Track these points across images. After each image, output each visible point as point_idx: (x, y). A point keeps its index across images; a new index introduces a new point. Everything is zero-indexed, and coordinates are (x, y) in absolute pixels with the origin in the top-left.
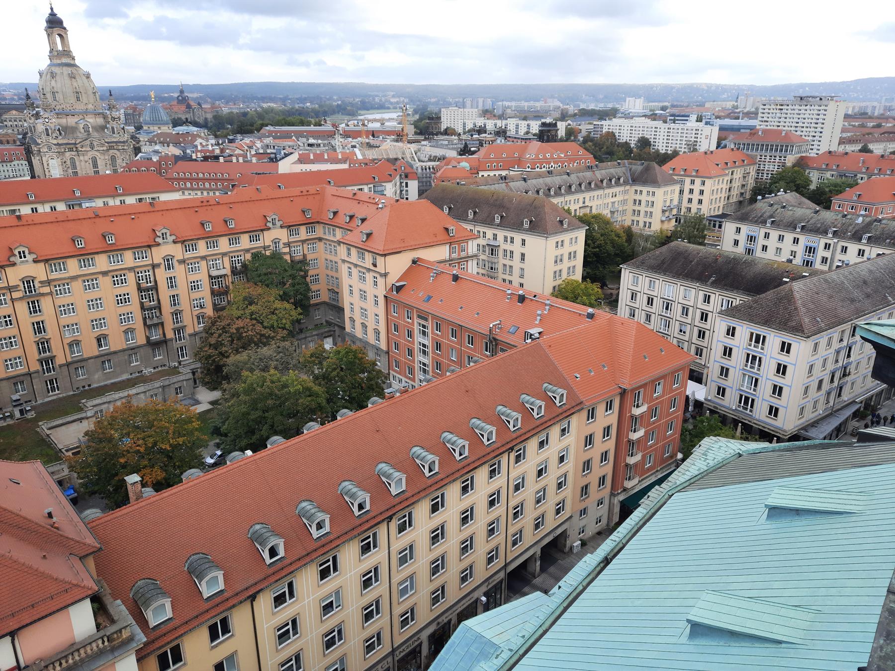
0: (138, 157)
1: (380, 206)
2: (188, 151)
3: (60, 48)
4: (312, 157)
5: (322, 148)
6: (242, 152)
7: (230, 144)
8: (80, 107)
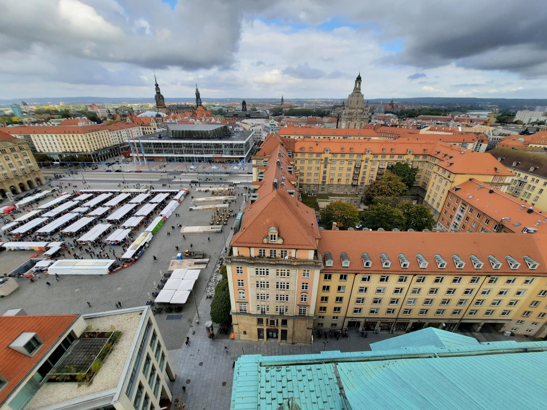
1: (462, 153)
2: (387, 123)
4: (436, 128)
5: (443, 125)
6: (407, 124)
8: (357, 106)
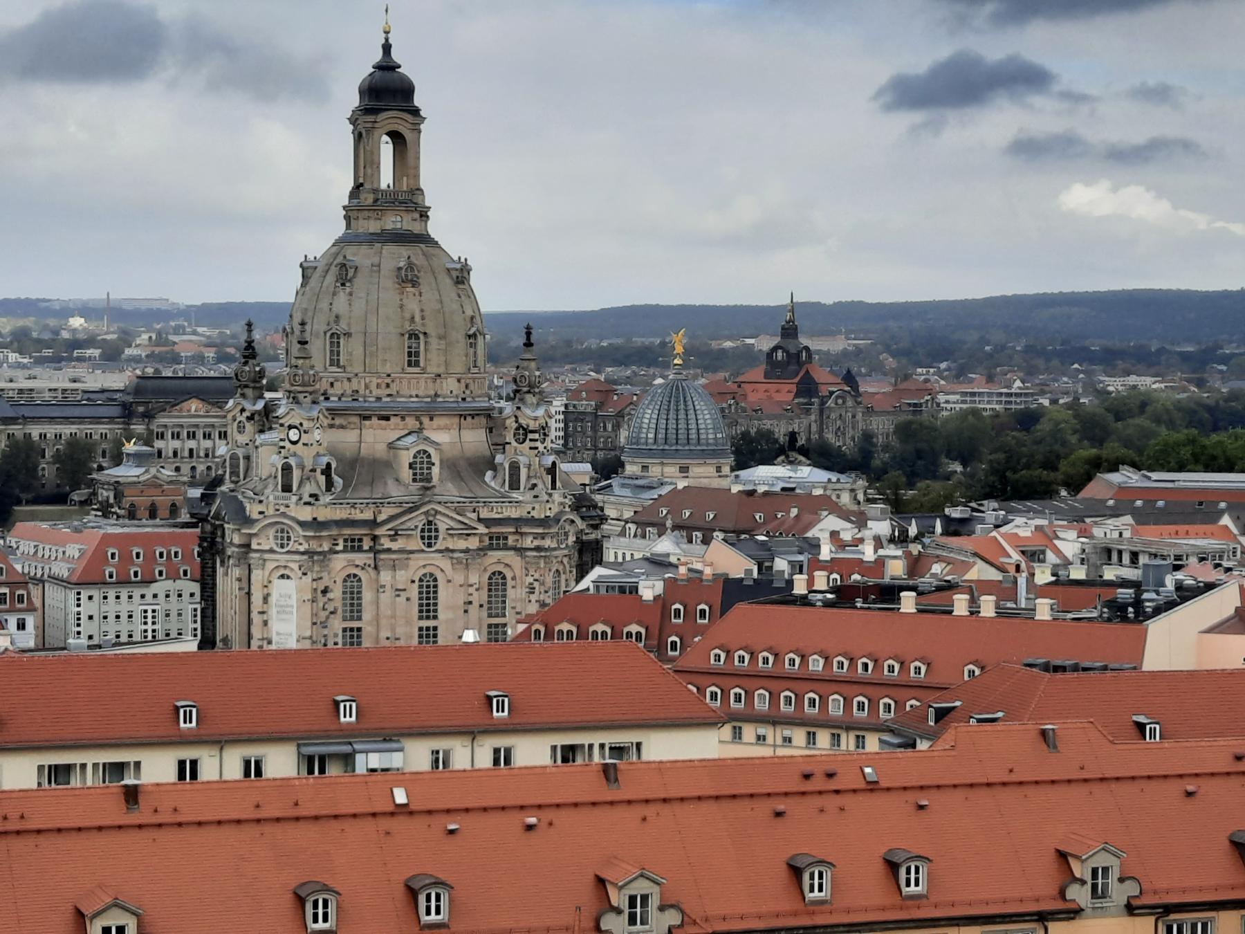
0: (587, 582)
2: (781, 564)
3: (386, 178)
6: (994, 575)
7: (954, 541)
8: (414, 388)
